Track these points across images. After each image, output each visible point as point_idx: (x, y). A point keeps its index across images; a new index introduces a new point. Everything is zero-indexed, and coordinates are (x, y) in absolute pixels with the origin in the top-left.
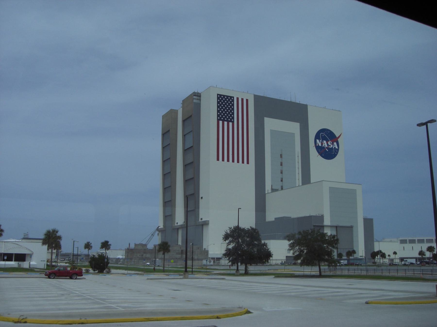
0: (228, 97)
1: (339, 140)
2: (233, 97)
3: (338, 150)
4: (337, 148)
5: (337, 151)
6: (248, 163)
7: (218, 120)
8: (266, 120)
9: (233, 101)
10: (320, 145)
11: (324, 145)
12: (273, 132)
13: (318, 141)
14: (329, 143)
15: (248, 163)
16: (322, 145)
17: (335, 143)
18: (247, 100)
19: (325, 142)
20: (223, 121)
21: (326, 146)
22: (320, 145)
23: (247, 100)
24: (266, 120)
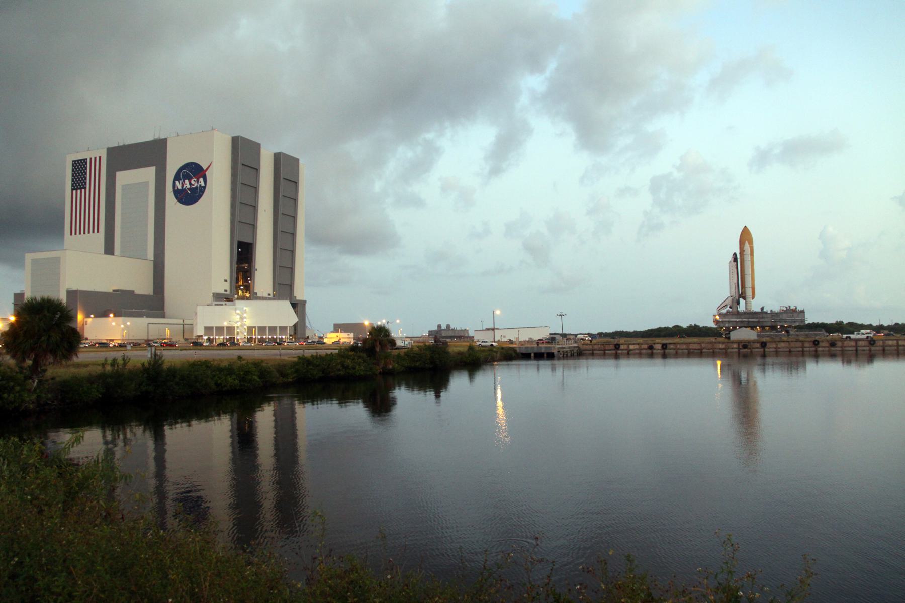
1: (207, 173)
3: (204, 188)
4: (203, 185)
5: (202, 190)
7: (72, 190)
8: (119, 175)
10: (180, 187)
12: (124, 187)
13: (177, 183)
14: (193, 182)
17: (201, 180)
18: (100, 158)
19: (187, 182)
20: (76, 190)
21: (188, 186)
22: (180, 187)
23: (100, 158)
24: (119, 175)
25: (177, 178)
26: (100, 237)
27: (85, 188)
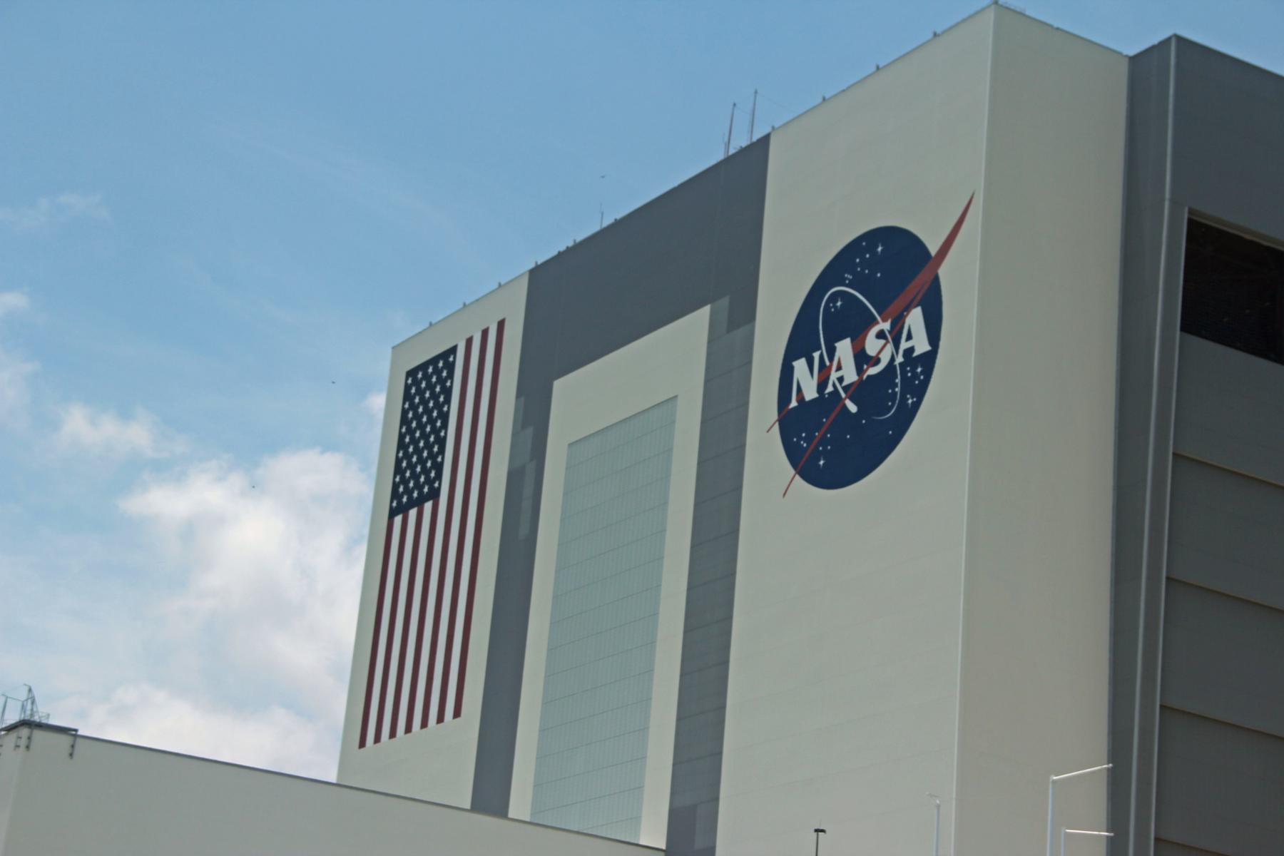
0: (434, 361)
1: (943, 272)
2: (453, 350)
3: (929, 360)
4: (921, 345)
6: (457, 713)
9: (451, 367)
10: (810, 393)
11: (834, 376)
13: (800, 365)
14: (872, 345)
15: (457, 713)
16: (822, 386)
17: (915, 319)
18: (501, 325)
19: (844, 348)
21: (851, 376)
23: (501, 325)
25: (801, 343)
26: (462, 735)
27: (434, 495)
